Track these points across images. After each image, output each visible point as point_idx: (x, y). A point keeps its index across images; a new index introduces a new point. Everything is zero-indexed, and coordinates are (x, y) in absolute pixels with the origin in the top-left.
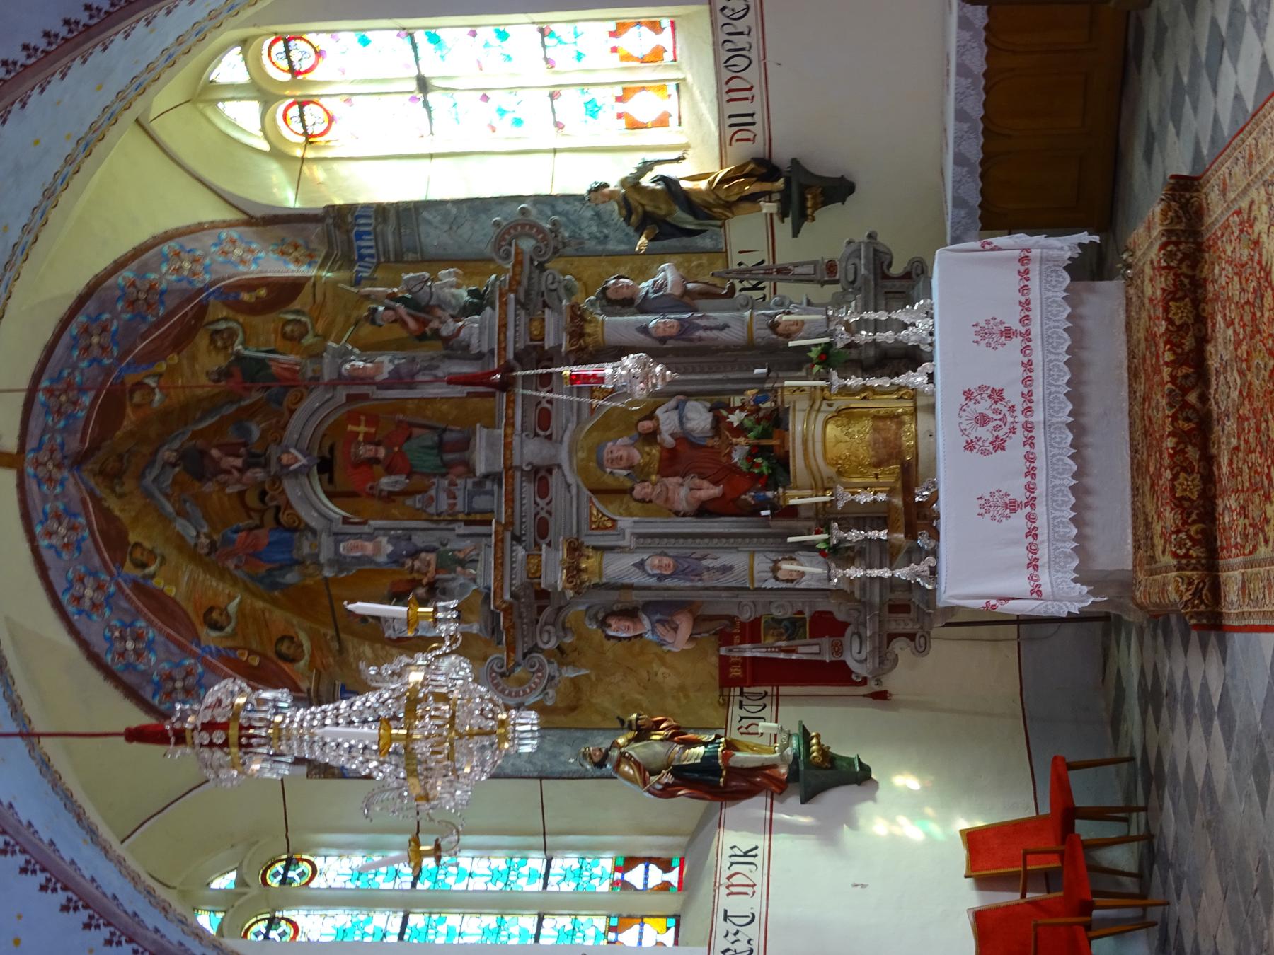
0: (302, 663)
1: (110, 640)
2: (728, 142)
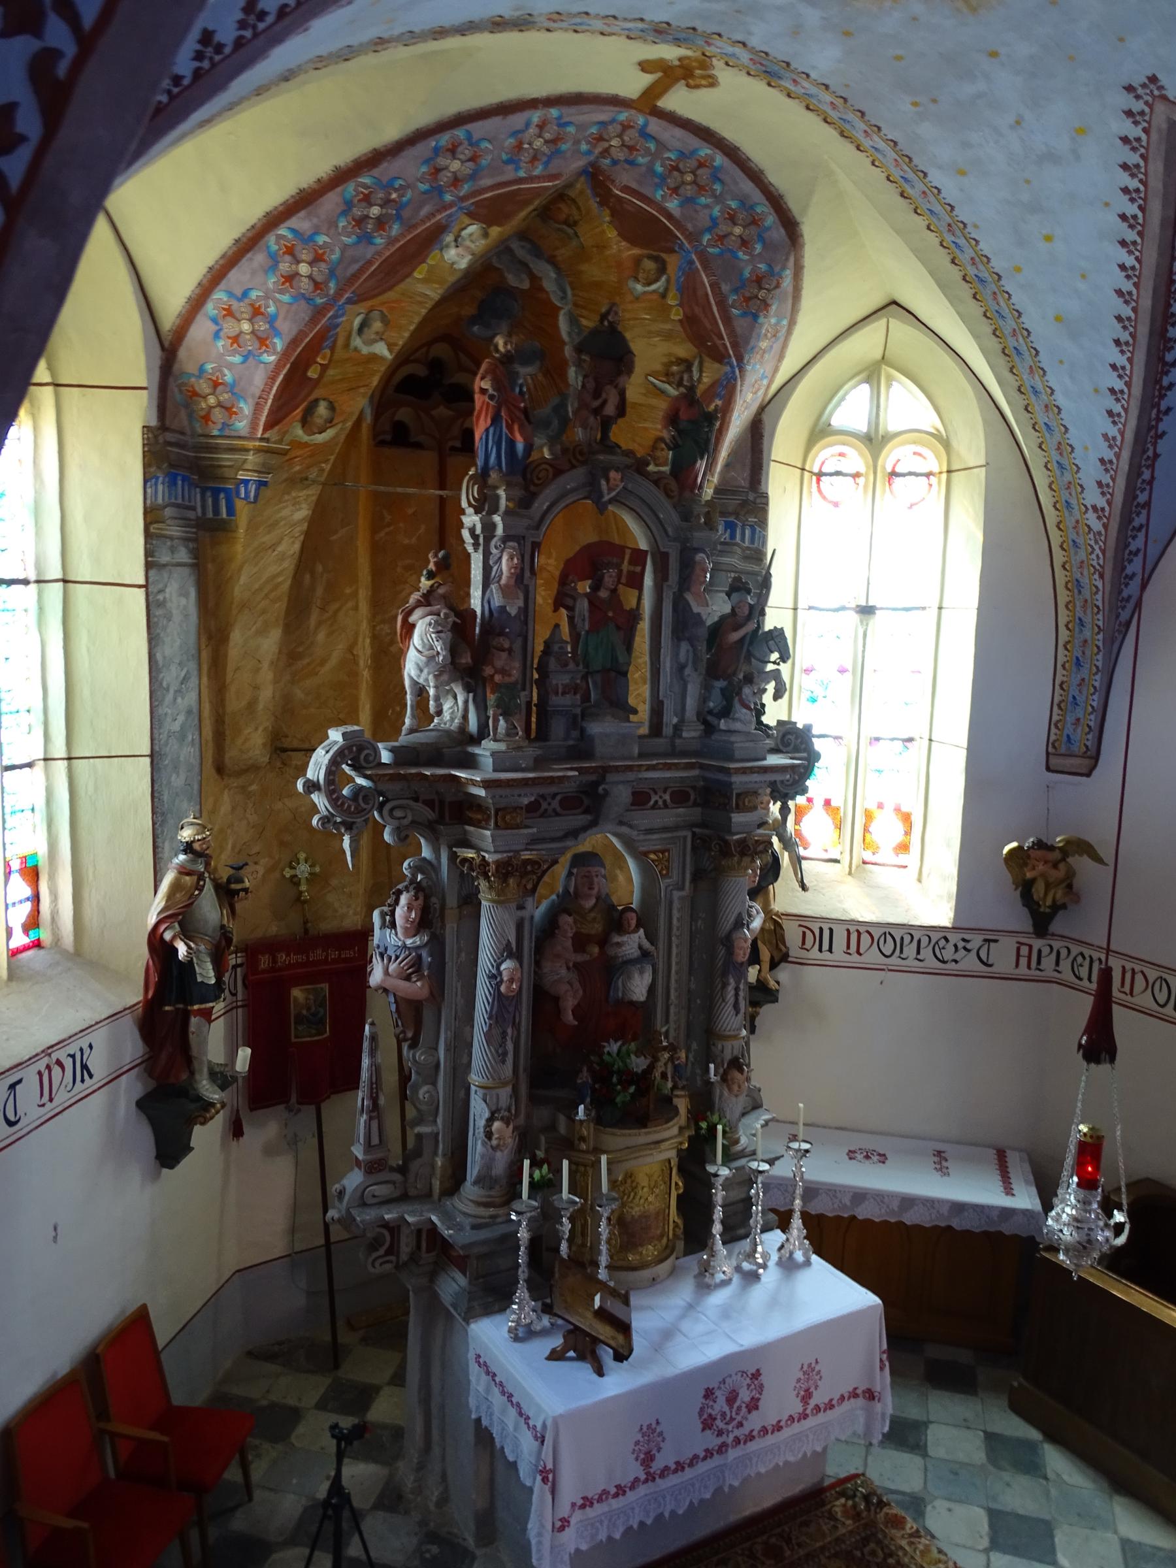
0: (299, 432)
1: (388, 187)
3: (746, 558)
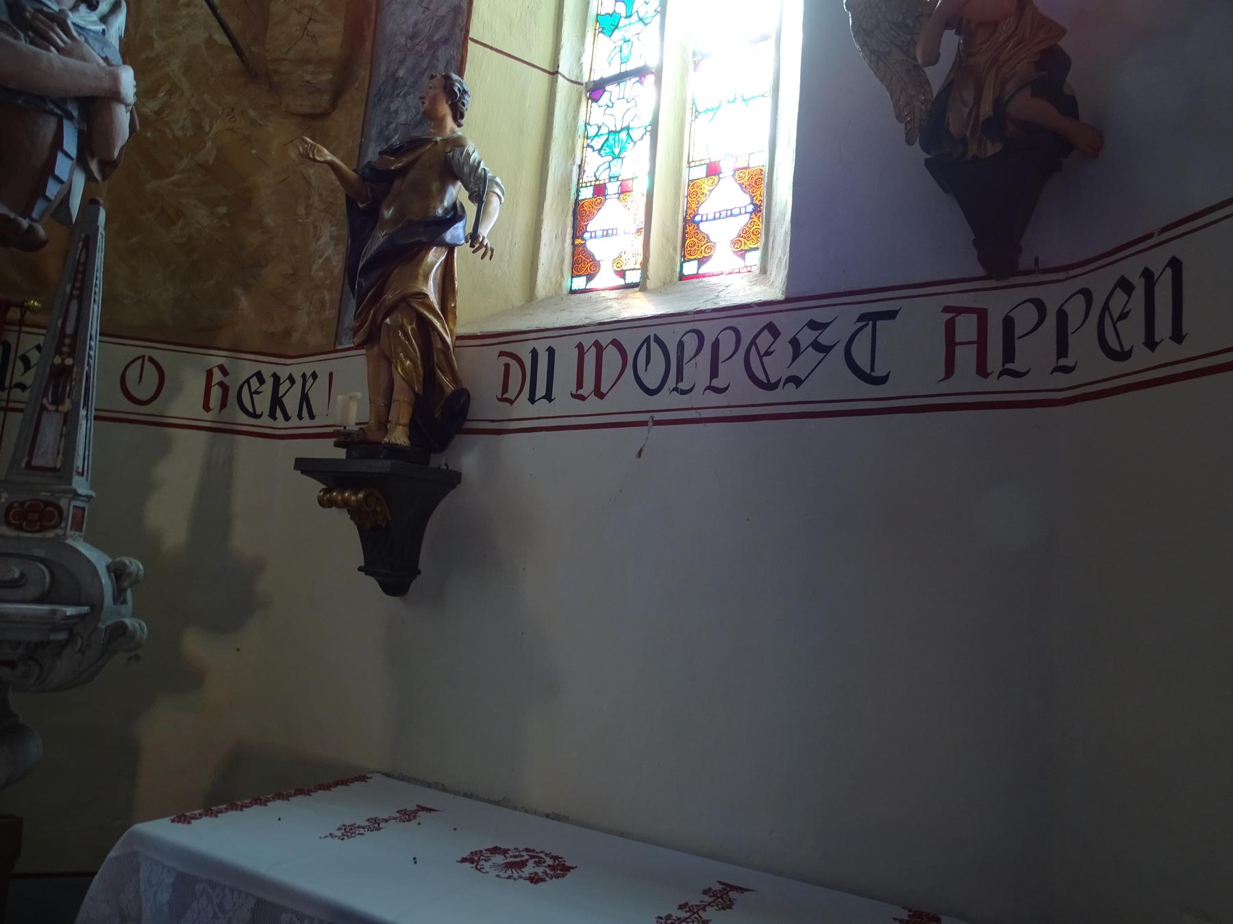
2: (506, 348)
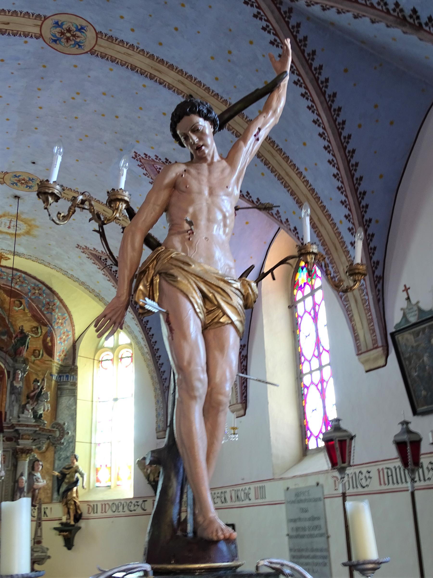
3: (72, 385)
